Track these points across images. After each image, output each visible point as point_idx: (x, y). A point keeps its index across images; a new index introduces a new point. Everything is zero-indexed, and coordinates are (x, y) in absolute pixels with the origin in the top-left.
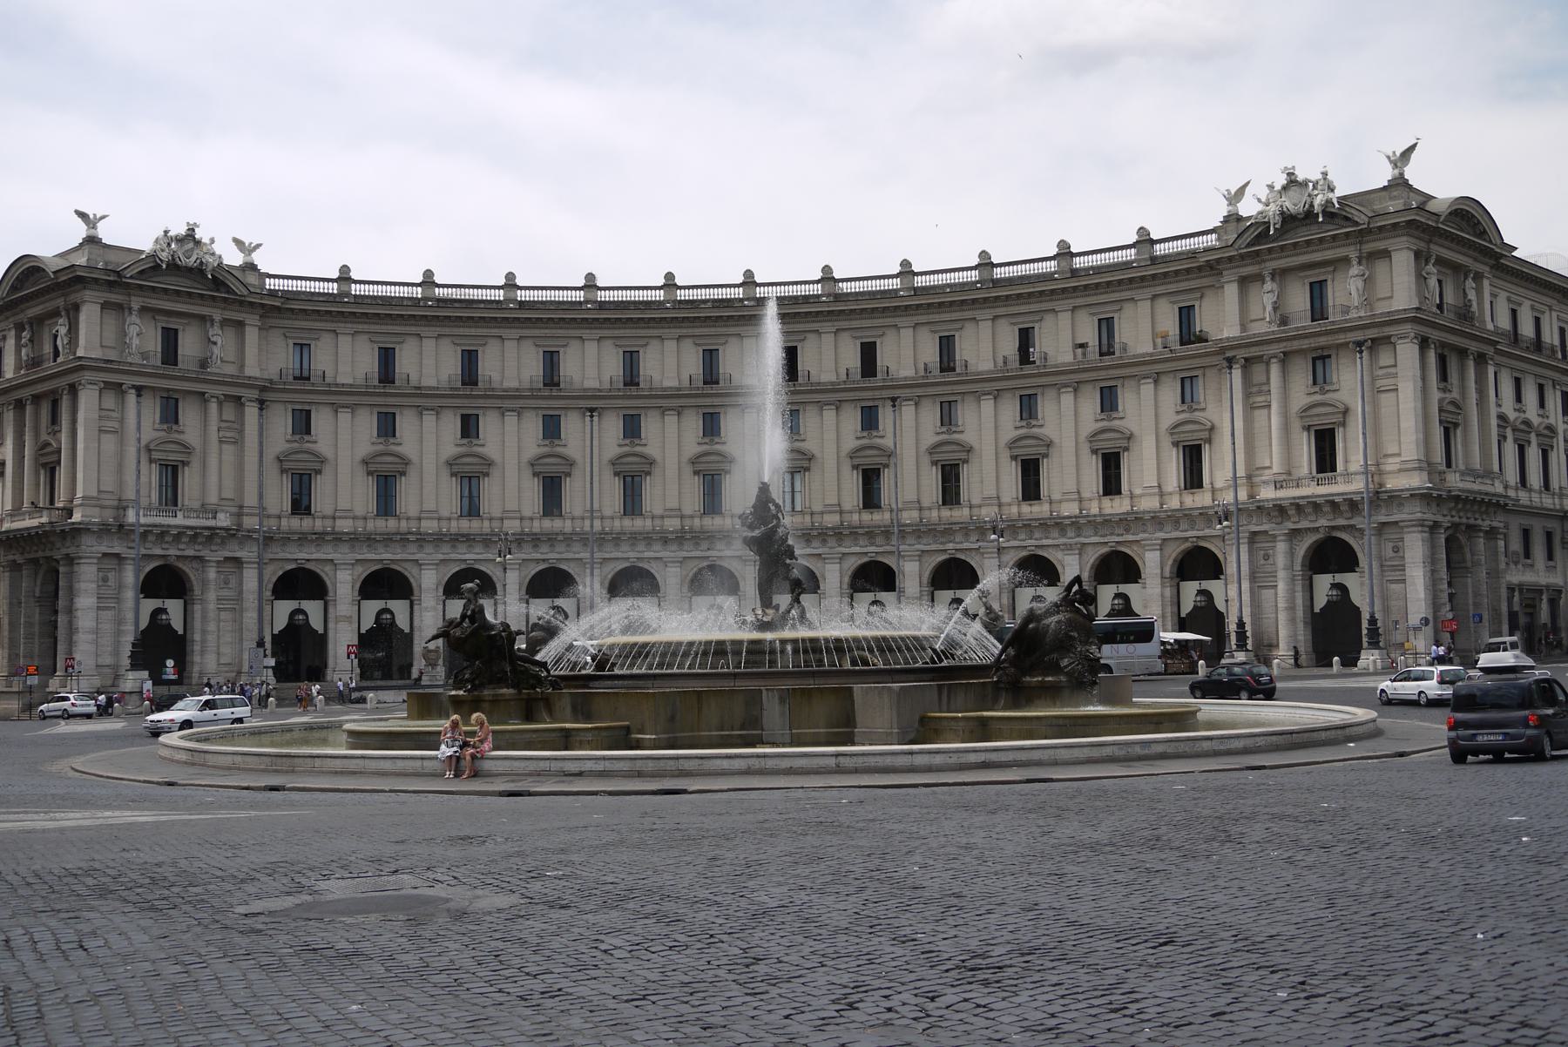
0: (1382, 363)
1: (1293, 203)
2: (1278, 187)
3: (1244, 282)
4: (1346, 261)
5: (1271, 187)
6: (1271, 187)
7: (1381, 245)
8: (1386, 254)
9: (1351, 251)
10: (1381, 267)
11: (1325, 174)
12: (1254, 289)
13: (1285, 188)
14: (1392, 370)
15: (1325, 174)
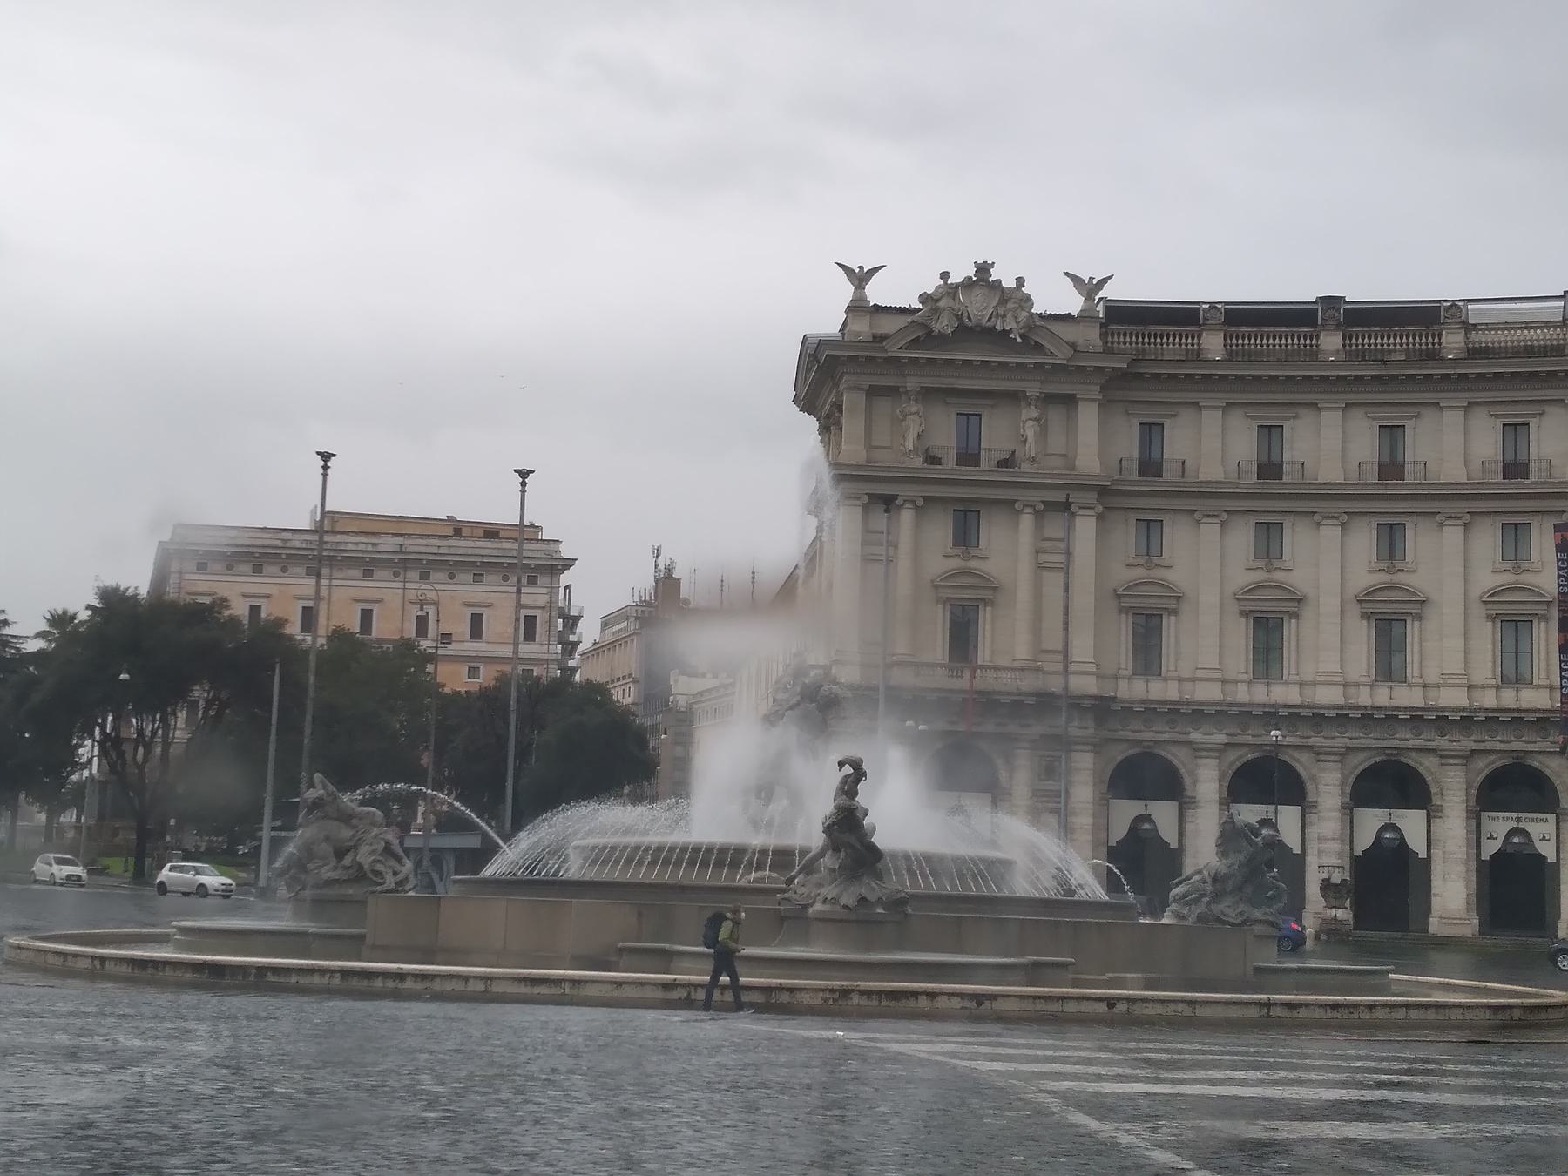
0: (1049, 533)
1: (979, 308)
2: (955, 279)
3: (873, 392)
4: (1015, 398)
5: (945, 276)
6: (945, 276)
7: (1066, 389)
8: (1070, 401)
9: (1033, 389)
10: (1056, 416)
11: (1020, 281)
12: (883, 406)
13: (968, 284)
14: (1062, 546)
15: (1020, 281)
